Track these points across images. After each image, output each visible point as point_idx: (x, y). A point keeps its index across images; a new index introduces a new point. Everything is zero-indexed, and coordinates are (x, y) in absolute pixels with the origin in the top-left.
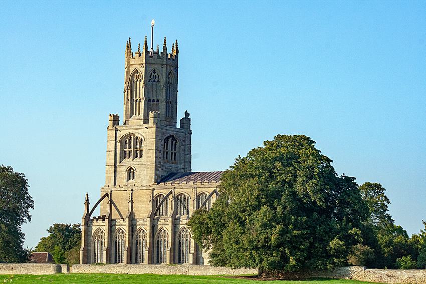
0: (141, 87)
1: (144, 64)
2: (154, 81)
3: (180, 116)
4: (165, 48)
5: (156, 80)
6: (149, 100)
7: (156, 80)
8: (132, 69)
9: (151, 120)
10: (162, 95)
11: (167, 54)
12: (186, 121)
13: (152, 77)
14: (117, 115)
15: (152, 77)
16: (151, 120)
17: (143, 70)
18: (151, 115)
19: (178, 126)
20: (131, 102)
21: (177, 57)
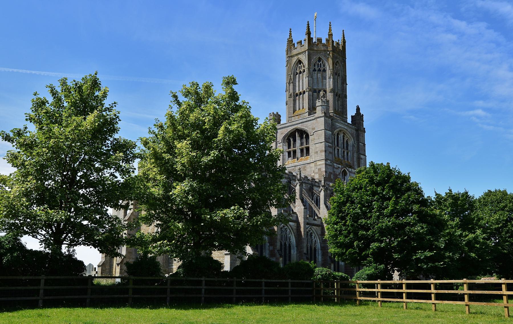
0: (304, 78)
1: (307, 52)
2: (319, 70)
3: (351, 112)
4: (331, 35)
5: (322, 69)
6: (315, 91)
7: (322, 69)
8: (295, 59)
9: (319, 111)
10: (329, 84)
11: (333, 41)
12: (358, 118)
13: (316, 66)
14: (277, 113)
15: (316, 66)
16: (319, 111)
17: (304, 59)
18: (318, 103)
19: (349, 121)
20: (295, 96)
21: (344, 47)
